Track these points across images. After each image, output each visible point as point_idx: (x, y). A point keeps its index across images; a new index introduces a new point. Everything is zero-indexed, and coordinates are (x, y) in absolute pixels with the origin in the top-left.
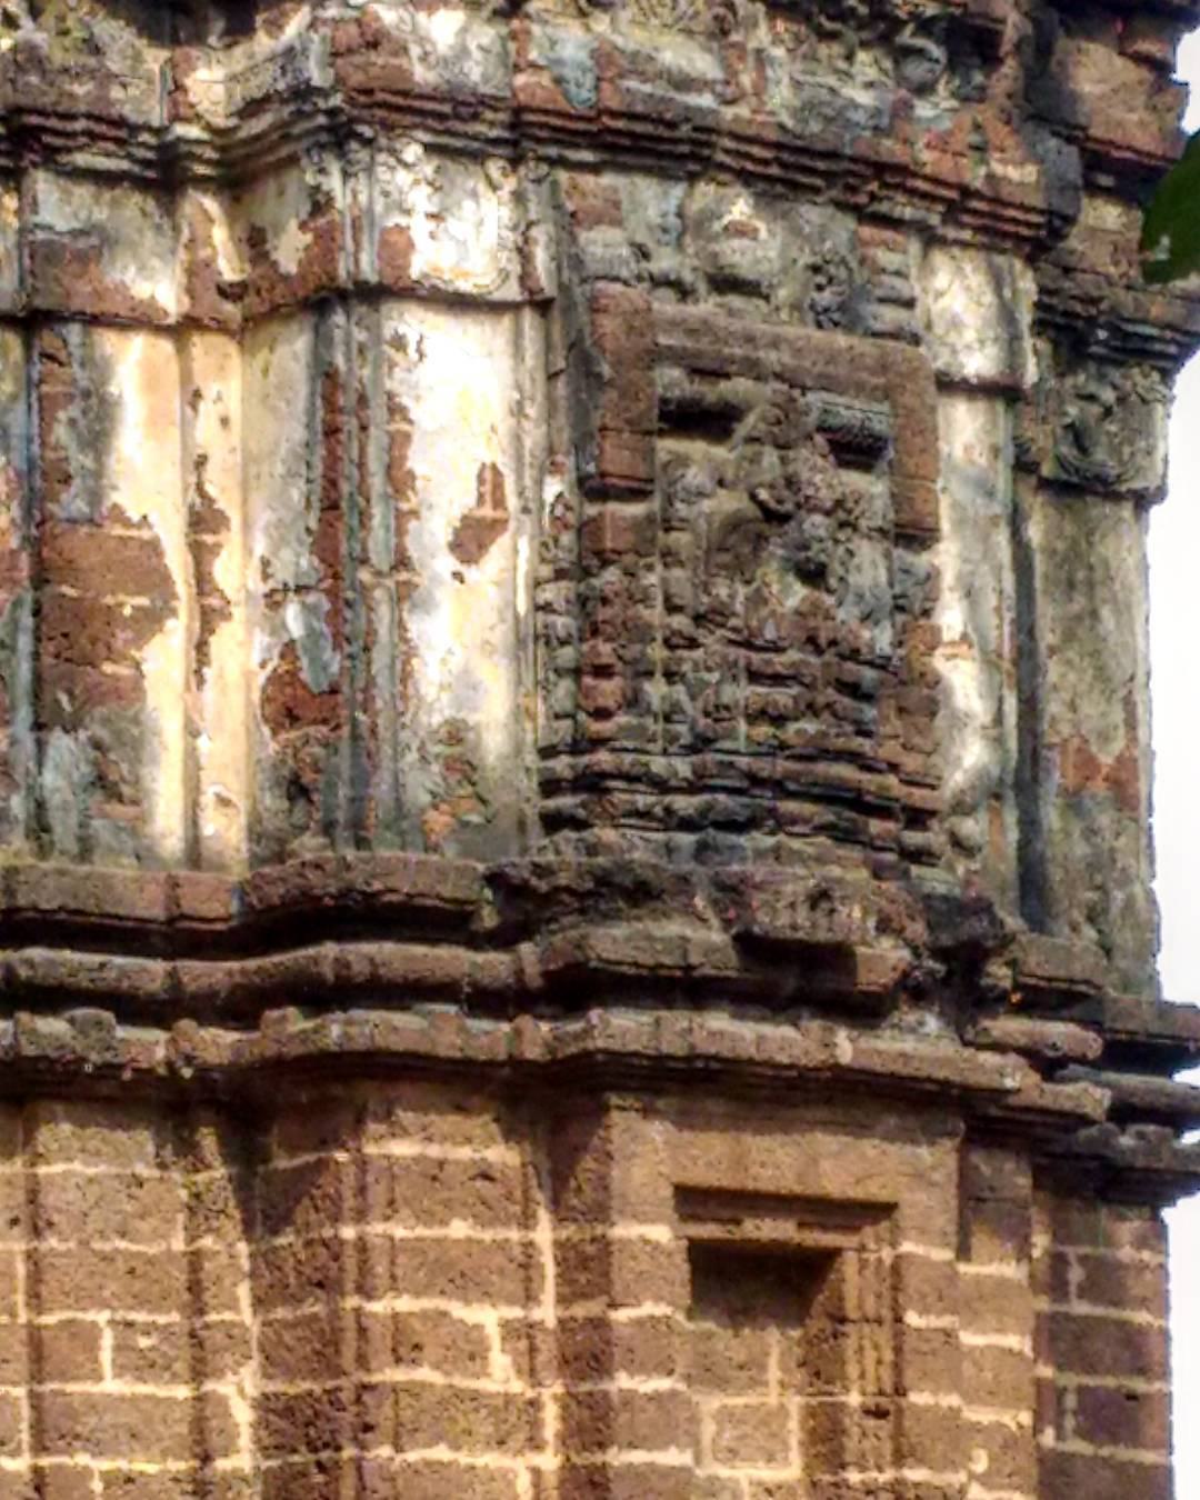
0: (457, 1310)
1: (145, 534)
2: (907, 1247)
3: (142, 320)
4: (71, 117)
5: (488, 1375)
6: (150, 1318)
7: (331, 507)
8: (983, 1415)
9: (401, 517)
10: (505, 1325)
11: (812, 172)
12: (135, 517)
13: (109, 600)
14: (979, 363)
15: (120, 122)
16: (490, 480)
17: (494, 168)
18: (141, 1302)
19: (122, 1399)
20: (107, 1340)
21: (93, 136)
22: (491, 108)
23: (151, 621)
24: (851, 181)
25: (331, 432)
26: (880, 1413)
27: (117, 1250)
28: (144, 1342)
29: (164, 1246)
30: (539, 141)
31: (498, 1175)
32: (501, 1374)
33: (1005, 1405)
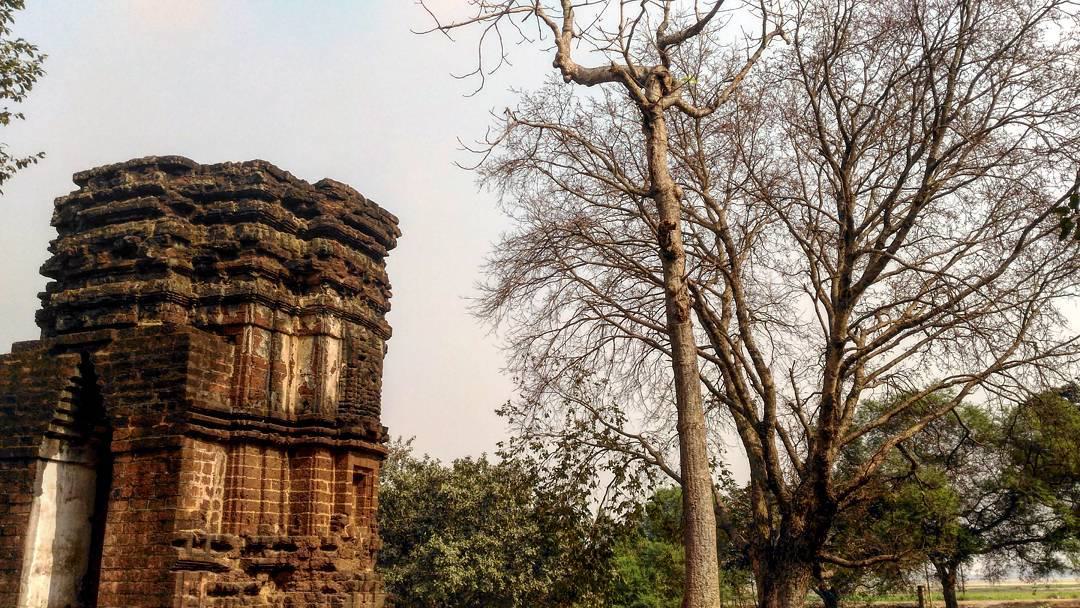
3: (286, 333)
7: (316, 363)
23: (284, 376)
25: (316, 353)
32: (328, 492)
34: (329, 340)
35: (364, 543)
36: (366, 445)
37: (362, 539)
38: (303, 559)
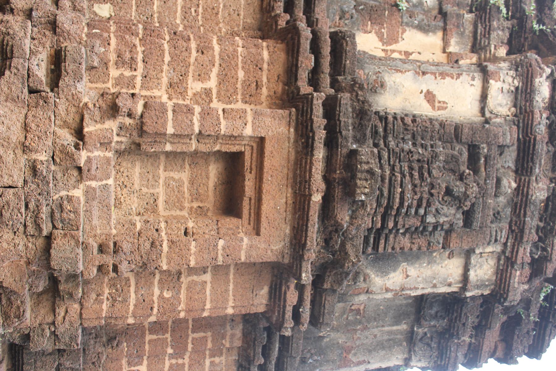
0: (215, 70)
1: (400, 39)
2: (246, 240)
3: (446, 43)
5: (194, 81)
6: (200, 14)
8: (183, 295)
9: (434, 74)
10: (210, 89)
12: (404, 36)
13: (385, 25)
14: (472, 274)
15: (489, 34)
17: (513, 109)
18: (205, 10)
21: (485, 29)
22: (530, 105)
24: (518, 223)
26: (186, 233)
27: (220, 4)
28: (193, 10)
29: (221, 21)
30: (524, 120)
31: (258, 91)
32: (194, 86)
33: (187, 304)
34: (478, 83)
35: (70, 199)
36: (320, 153)
37: (78, 193)
38: (29, 14)
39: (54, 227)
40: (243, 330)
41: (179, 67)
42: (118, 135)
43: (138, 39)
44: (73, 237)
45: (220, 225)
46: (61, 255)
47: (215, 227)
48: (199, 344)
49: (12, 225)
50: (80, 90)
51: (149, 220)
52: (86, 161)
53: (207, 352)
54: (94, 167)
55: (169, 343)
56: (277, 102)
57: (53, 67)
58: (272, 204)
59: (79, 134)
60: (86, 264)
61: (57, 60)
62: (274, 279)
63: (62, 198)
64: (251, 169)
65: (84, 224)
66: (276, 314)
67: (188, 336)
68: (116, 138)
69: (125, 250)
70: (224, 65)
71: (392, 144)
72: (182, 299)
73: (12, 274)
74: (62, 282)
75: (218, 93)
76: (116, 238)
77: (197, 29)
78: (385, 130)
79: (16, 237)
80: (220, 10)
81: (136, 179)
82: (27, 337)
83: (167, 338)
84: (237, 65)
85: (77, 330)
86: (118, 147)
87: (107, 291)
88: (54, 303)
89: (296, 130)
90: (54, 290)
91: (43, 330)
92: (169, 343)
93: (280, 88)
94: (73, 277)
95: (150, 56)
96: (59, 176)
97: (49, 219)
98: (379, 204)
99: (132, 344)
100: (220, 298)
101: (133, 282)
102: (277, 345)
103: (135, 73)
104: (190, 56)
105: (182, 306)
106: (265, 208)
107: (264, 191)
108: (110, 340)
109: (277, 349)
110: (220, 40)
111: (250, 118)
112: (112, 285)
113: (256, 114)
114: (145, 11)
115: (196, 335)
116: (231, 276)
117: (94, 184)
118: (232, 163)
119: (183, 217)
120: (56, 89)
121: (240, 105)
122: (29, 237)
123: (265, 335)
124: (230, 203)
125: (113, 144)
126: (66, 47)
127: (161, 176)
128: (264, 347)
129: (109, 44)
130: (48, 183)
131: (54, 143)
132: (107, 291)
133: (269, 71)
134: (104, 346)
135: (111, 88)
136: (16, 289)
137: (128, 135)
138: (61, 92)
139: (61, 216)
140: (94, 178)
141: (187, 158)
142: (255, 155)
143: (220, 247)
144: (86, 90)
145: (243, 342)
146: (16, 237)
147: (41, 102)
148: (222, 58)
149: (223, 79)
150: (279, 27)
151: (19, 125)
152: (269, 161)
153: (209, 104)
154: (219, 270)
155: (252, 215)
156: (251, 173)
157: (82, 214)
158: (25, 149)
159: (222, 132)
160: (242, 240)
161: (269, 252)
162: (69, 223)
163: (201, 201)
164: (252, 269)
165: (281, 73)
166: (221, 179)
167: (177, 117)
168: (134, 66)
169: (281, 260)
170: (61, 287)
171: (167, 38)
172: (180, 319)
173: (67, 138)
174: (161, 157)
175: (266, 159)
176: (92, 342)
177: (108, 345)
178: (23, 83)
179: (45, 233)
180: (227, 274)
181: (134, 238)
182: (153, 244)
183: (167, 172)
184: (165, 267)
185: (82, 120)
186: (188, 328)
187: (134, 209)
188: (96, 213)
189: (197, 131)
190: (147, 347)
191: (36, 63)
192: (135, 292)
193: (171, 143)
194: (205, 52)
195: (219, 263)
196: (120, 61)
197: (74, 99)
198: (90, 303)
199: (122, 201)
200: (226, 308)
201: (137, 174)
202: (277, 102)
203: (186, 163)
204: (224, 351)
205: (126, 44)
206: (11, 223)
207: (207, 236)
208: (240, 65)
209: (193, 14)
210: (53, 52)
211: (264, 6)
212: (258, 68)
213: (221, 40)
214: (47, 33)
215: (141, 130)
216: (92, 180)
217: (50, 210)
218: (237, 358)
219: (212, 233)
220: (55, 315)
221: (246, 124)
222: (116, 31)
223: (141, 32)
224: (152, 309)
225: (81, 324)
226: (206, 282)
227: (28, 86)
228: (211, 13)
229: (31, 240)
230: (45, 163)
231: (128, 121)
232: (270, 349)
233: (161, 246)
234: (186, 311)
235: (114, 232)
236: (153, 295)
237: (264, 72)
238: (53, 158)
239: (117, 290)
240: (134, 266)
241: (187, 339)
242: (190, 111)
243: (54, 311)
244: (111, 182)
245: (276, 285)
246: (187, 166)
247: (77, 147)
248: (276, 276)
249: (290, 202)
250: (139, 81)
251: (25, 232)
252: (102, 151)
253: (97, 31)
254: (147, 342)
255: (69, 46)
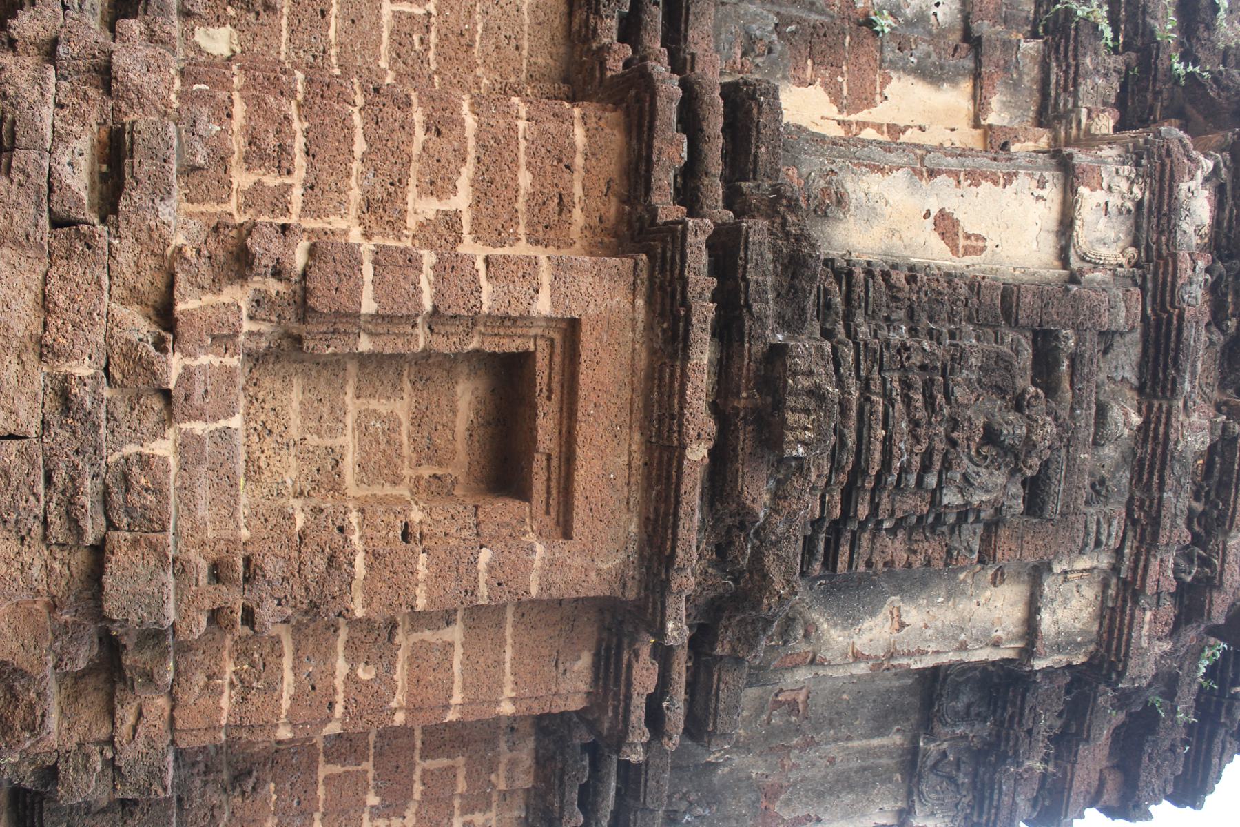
0: (467, 172)
1: (878, 98)
2: (539, 548)
4: (1075, 57)
8: (400, 676)
10: (457, 214)
11: (1151, 474)
12: (886, 92)
13: (844, 68)
16: (976, 244)
17: (1131, 250)
18: (443, 38)
19: (379, 18)
20: (419, 11)
21: (1066, 72)
22: (1168, 240)
24: (1147, 503)
26: (406, 536)
27: (476, 24)
28: (416, 38)
29: (479, 62)
30: (1155, 274)
32: (422, 208)
33: (410, 694)
34: (1052, 193)
35: (145, 462)
36: (703, 354)
37: (163, 448)
38: (49, 50)
39: (111, 525)
40: (536, 751)
41: (387, 166)
42: (252, 318)
43: (294, 103)
44: (152, 546)
45: (481, 517)
46: (126, 587)
47: (471, 521)
48: (438, 784)
49: (17, 522)
50: (166, 218)
51: (323, 506)
52: (181, 377)
53: (457, 803)
54: (199, 390)
55: (371, 782)
56: (606, 240)
57: (104, 168)
58: (597, 466)
59: (165, 316)
60: (183, 607)
61: (115, 153)
62: (605, 635)
63: (127, 460)
64: (550, 391)
65: (178, 518)
66: (610, 714)
67: (412, 766)
68: (247, 326)
69: (270, 575)
70: (486, 160)
71: (864, 330)
72: (399, 684)
73: (16, 631)
74: (130, 648)
75: (475, 221)
76: (250, 549)
77: (425, 81)
78: (848, 300)
79: (26, 549)
80: (477, 38)
81: (293, 416)
82: (50, 774)
83: (366, 772)
84: (516, 159)
85: (164, 756)
86: (253, 345)
87: (230, 668)
88: (111, 697)
89: (649, 302)
90: (113, 664)
91: (87, 757)
92: (371, 782)
93: (613, 211)
94: (154, 637)
95: (321, 141)
96: (121, 410)
97: (99, 508)
98: (836, 466)
99: (288, 785)
100: (484, 680)
101: (288, 646)
102: (613, 784)
103: (288, 181)
104: (411, 141)
105: (399, 700)
106: (582, 476)
107: (580, 439)
108: (239, 777)
109: (613, 793)
110: (476, 106)
111: (545, 278)
112: (242, 653)
113: (560, 267)
114: (309, 42)
115: (431, 764)
116: (509, 631)
117: (198, 427)
118: (508, 377)
119: (400, 499)
120: (112, 217)
121: (523, 249)
122: (54, 548)
123: (586, 762)
124: (505, 465)
125: (241, 338)
126: (134, 122)
127: (350, 408)
128: (583, 790)
129: (229, 116)
130: (96, 427)
131: (109, 337)
132: (230, 668)
133: (587, 171)
134: (225, 790)
135: (235, 213)
136: (25, 666)
137: (274, 318)
138: (123, 224)
139: (125, 500)
140: (200, 415)
141: (406, 367)
142: (557, 359)
143: (482, 565)
144: (180, 220)
145: (536, 777)
146: (26, 549)
147: (80, 247)
148: (481, 144)
149: (484, 190)
150: (609, 74)
151: (30, 297)
152: (591, 372)
153: (454, 247)
154: (482, 618)
155: (554, 492)
156: (549, 398)
157: (172, 494)
158: (45, 351)
159: (485, 309)
160: (532, 548)
161: (593, 575)
162: (143, 516)
163: (440, 464)
164: (555, 614)
165: (615, 176)
166: (482, 413)
167: (383, 277)
168: (286, 164)
169: (619, 594)
170: (127, 661)
171: (360, 100)
172: (395, 729)
173: (138, 325)
174: (349, 366)
175: (583, 367)
176: (198, 782)
177: (234, 788)
178: (38, 206)
179: (90, 539)
180: (500, 626)
181: (290, 548)
182: (331, 560)
183: (362, 400)
184: (360, 613)
185: (171, 284)
186: (413, 748)
187: (289, 482)
188: (203, 492)
189: (428, 305)
190: (321, 792)
191: (66, 160)
192: (293, 669)
193: (371, 334)
194: (444, 131)
195: (481, 602)
196: (255, 154)
197: (154, 239)
198: (192, 694)
199: (262, 464)
200: (497, 702)
201: (296, 405)
202: (606, 240)
203: (405, 379)
204: (495, 798)
205: (268, 115)
206: (14, 516)
207: (453, 542)
208: (523, 159)
209: (417, 46)
210: (104, 134)
211: (575, 27)
212: (562, 165)
213: (480, 104)
214: (92, 92)
215: (303, 306)
216: (195, 419)
217: (101, 488)
218: (523, 815)
219: (465, 534)
220: (114, 724)
221: (537, 291)
222: (246, 87)
223: (300, 87)
224: (331, 705)
225: (173, 742)
226: (451, 645)
227: (50, 210)
228: (456, 45)
229: (59, 555)
230: (88, 381)
231: (273, 286)
232: (597, 793)
233: (351, 564)
234: (407, 710)
235: (245, 534)
236: (333, 675)
237: (576, 175)
238: (106, 370)
239: (252, 665)
240: (290, 611)
241: (412, 772)
242: (412, 262)
243: (111, 713)
244: (236, 422)
245: (608, 649)
246: (407, 386)
247: (160, 345)
248: (609, 629)
249: (637, 462)
250: (297, 193)
251: (45, 538)
252: (218, 355)
253: (203, 87)
254: (321, 780)
255: (140, 120)
